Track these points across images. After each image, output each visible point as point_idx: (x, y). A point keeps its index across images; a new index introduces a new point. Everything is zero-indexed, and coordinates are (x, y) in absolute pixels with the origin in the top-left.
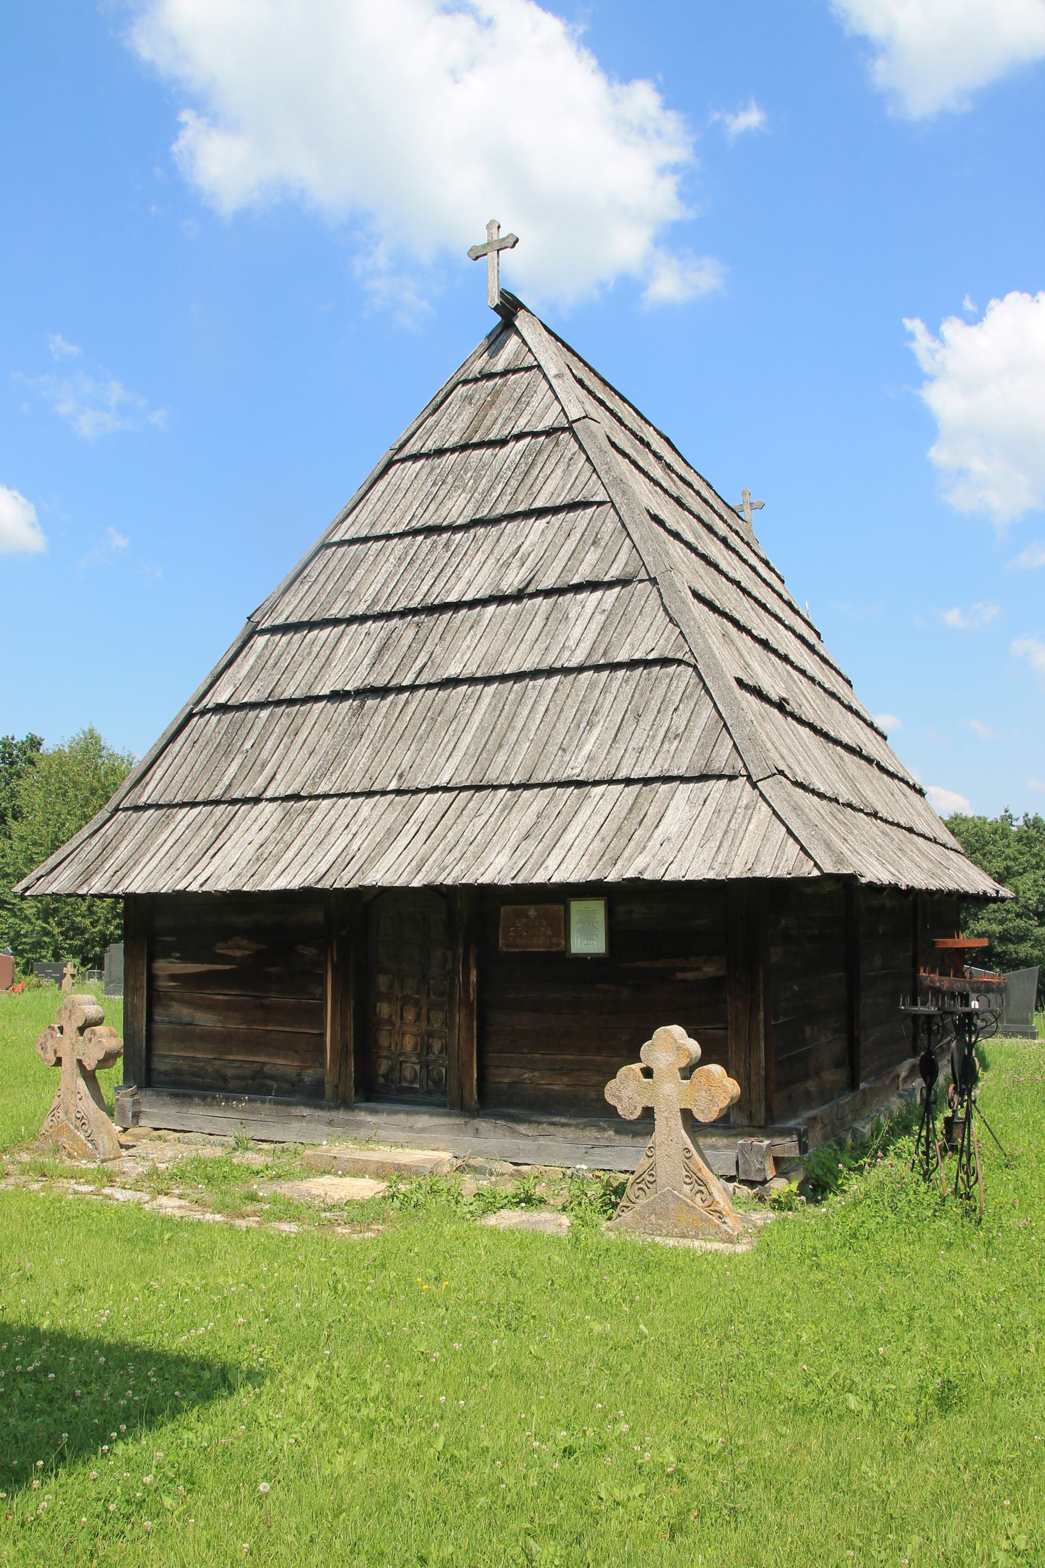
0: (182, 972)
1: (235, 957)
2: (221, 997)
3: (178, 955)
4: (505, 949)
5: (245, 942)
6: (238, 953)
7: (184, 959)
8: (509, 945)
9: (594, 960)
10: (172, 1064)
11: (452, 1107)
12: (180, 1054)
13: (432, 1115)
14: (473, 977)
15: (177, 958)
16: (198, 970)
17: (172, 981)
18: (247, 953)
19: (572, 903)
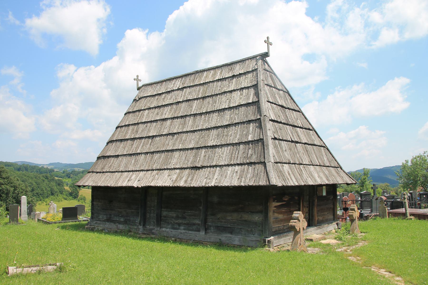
0: (277, 205)
1: (285, 200)
2: (284, 210)
3: (276, 201)
4: (318, 195)
5: (287, 197)
6: (286, 199)
7: (277, 202)
8: (319, 195)
9: (325, 196)
10: (275, 229)
11: (314, 226)
12: (276, 226)
13: (312, 227)
14: (316, 201)
15: (276, 202)
16: (279, 204)
17: (275, 208)
18: (288, 199)
19: (323, 187)
